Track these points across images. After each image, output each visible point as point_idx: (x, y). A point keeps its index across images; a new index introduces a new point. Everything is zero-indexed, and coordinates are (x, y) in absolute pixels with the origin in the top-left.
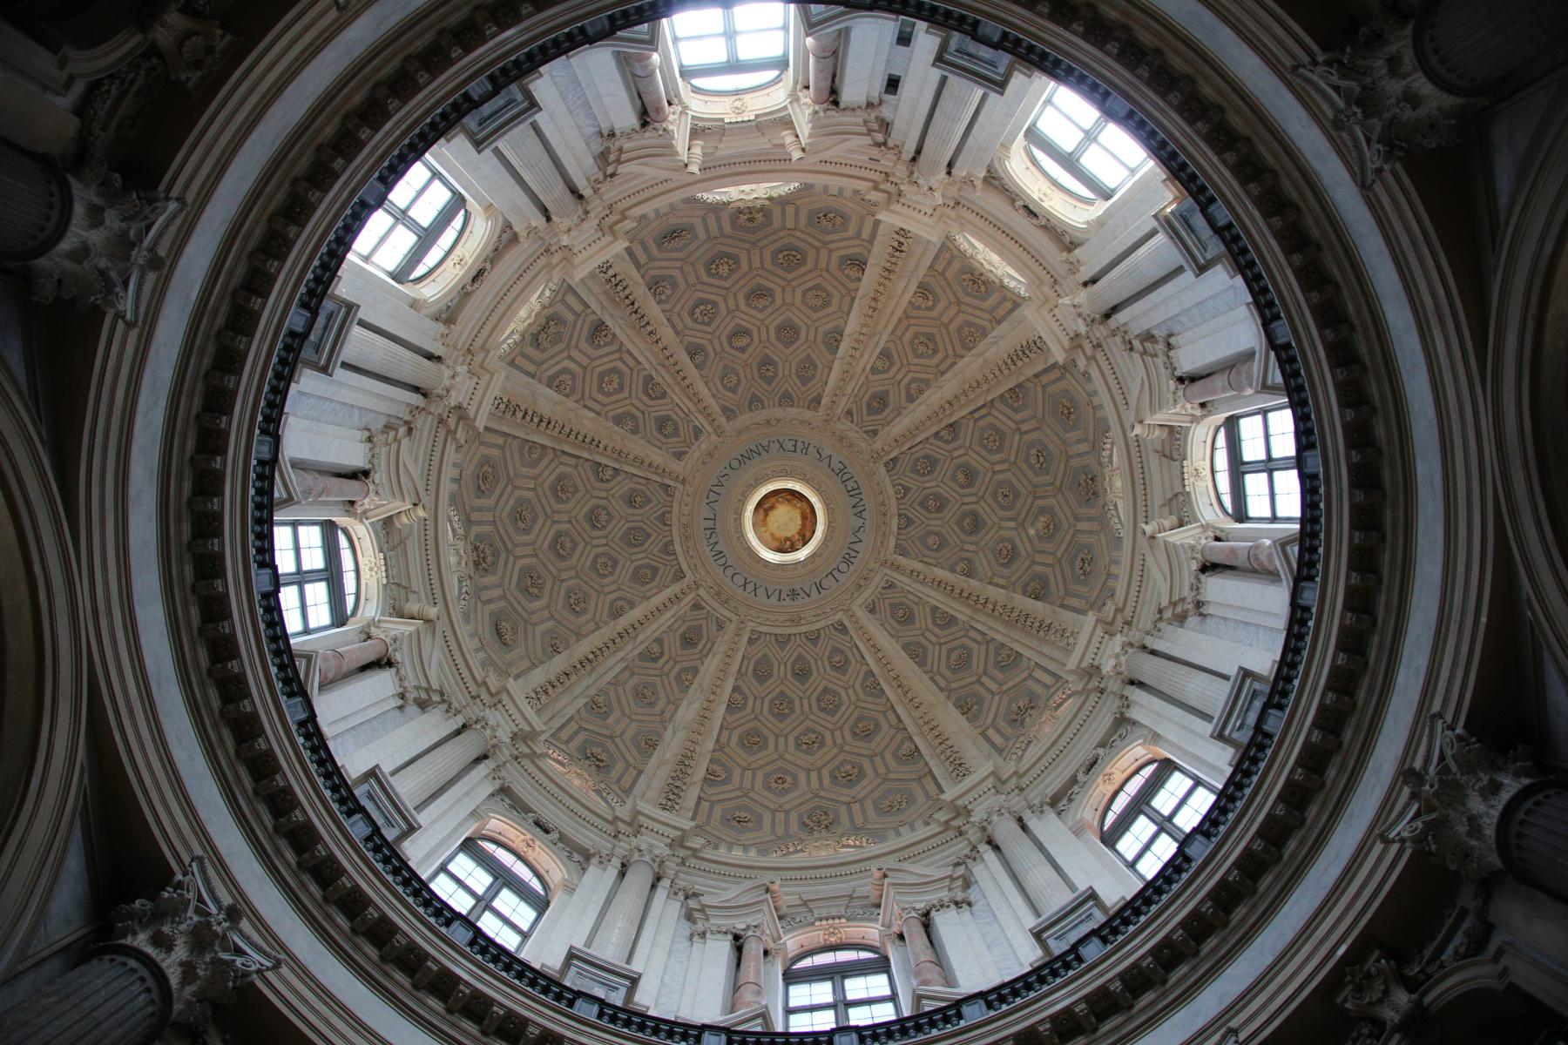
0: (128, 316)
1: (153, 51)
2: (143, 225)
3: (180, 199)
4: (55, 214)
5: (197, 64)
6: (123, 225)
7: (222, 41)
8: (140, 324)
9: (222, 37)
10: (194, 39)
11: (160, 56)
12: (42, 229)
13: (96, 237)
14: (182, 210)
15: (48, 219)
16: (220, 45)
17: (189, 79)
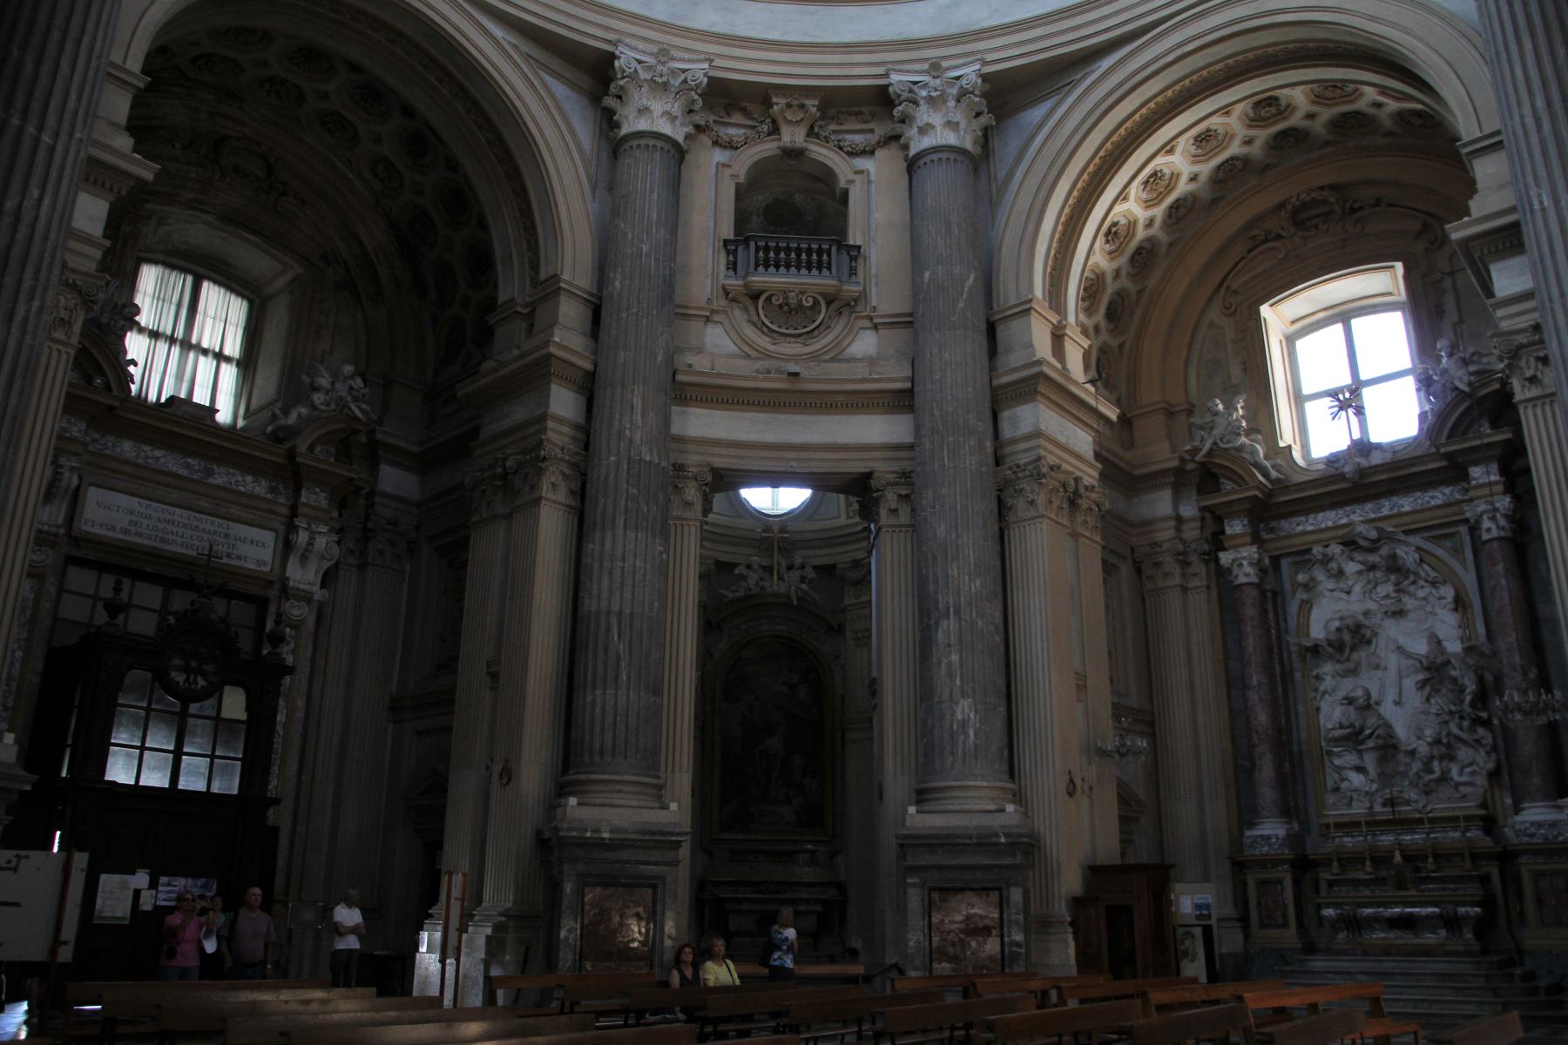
0: (978, 67)
1: (811, 133)
2: (915, 88)
3: (886, 75)
4: (935, 157)
5: (802, 106)
6: (922, 102)
7: (779, 102)
8: (979, 56)
9: (777, 104)
10: (790, 118)
11: (812, 127)
12: (948, 159)
13: (937, 119)
14: (894, 70)
15: (940, 159)
16: (783, 101)
17: (813, 106)
